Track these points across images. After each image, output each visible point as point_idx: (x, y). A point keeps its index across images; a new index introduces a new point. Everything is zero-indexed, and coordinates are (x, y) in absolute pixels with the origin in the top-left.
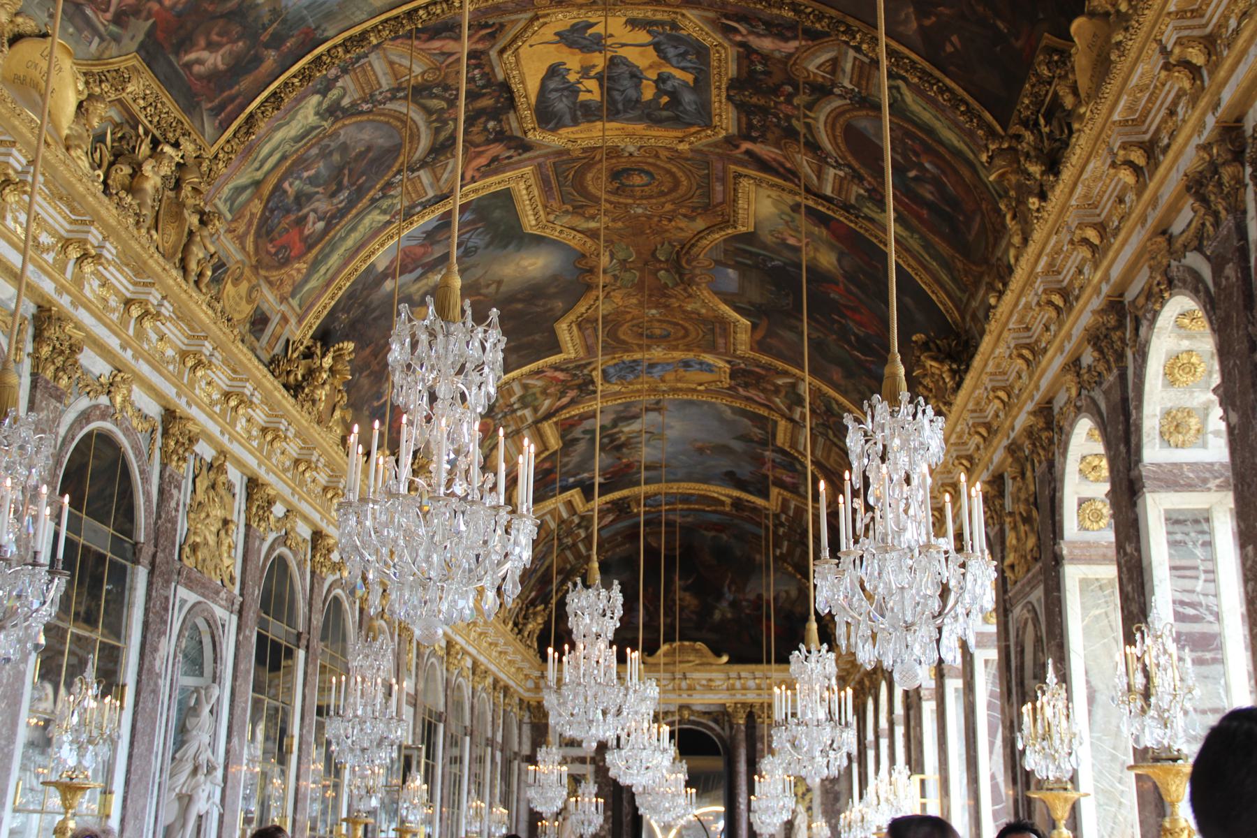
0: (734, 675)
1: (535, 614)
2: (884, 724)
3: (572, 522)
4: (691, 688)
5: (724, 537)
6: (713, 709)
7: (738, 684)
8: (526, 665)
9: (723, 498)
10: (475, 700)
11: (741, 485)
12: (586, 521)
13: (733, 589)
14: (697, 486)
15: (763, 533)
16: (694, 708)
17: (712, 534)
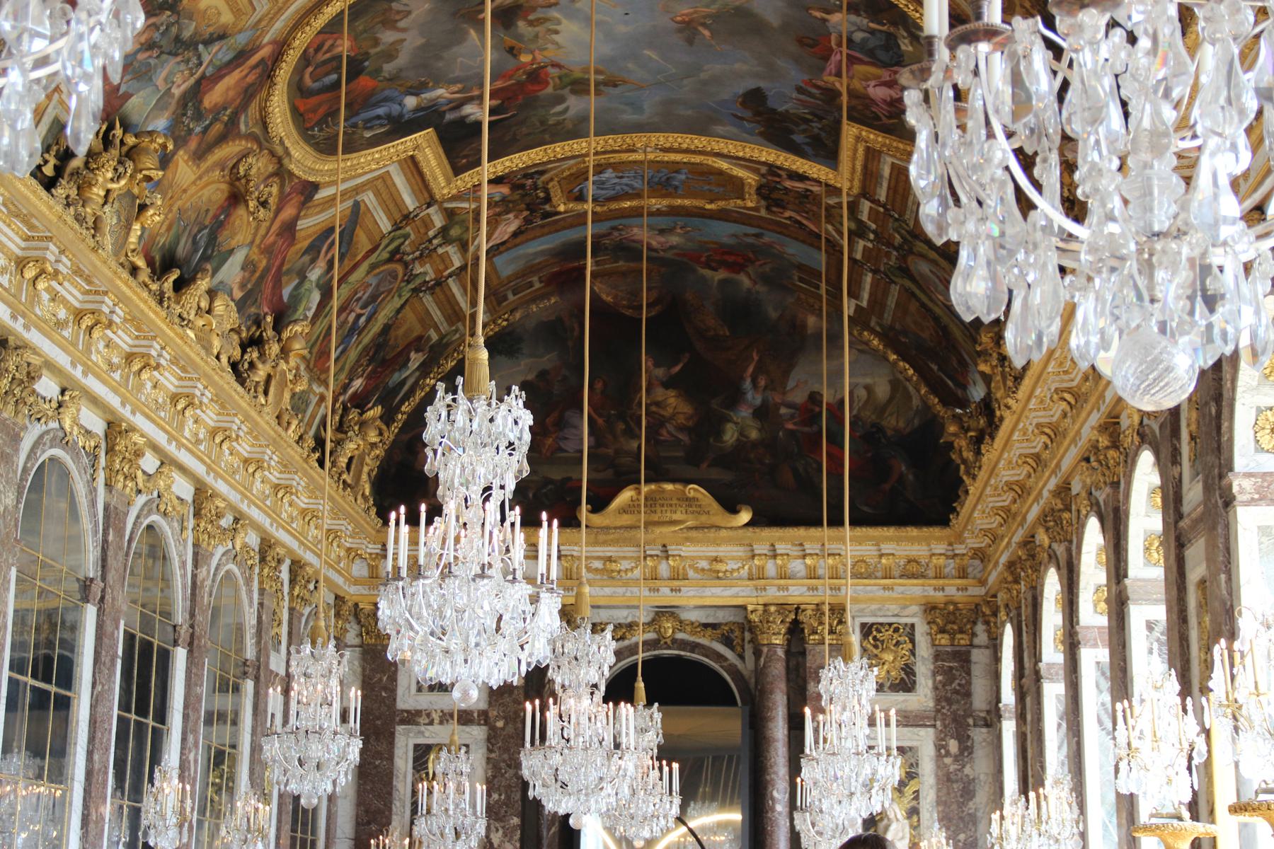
0: (762, 548)
1: (363, 424)
2: (1092, 616)
3: (427, 223)
4: (677, 576)
5: (745, 281)
6: (721, 617)
7: (771, 568)
8: (345, 526)
9: (739, 172)
10: (202, 573)
11: (776, 129)
12: (457, 226)
13: (762, 383)
14: (686, 140)
15: (821, 260)
16: (685, 616)
17: (721, 274)
